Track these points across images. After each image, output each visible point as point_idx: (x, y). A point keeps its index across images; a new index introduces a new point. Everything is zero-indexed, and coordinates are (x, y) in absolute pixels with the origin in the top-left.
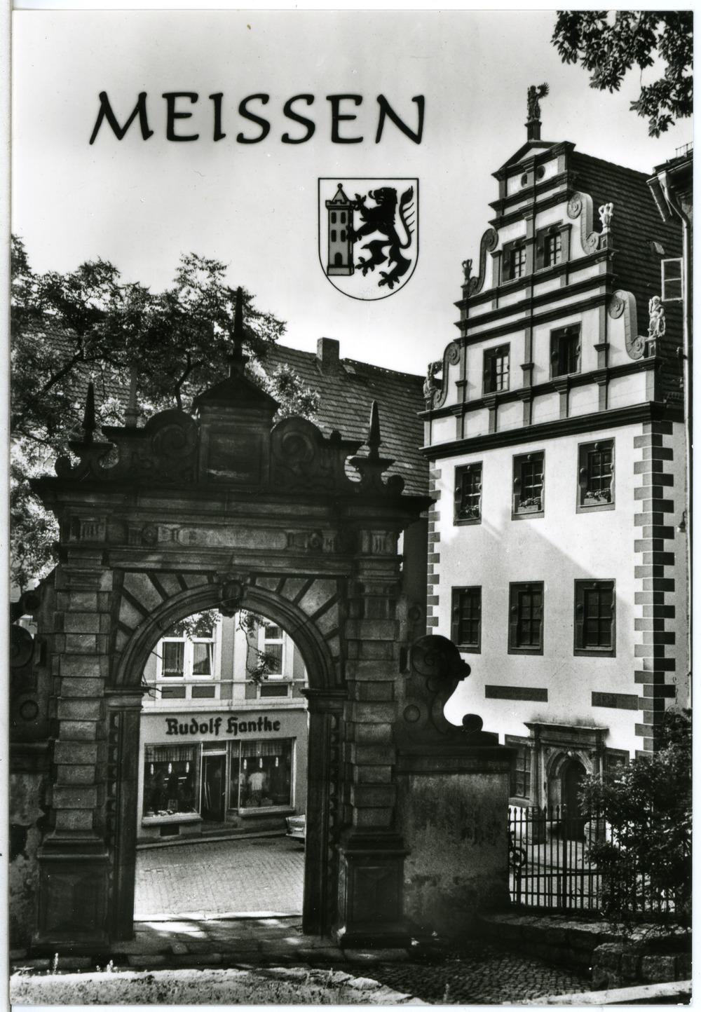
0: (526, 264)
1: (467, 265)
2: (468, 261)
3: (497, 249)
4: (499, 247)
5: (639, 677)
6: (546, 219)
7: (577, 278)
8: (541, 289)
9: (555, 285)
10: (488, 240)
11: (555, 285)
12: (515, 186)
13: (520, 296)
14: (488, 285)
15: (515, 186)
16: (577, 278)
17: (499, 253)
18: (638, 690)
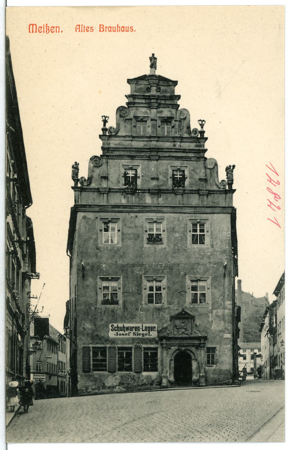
2: (107, 117)
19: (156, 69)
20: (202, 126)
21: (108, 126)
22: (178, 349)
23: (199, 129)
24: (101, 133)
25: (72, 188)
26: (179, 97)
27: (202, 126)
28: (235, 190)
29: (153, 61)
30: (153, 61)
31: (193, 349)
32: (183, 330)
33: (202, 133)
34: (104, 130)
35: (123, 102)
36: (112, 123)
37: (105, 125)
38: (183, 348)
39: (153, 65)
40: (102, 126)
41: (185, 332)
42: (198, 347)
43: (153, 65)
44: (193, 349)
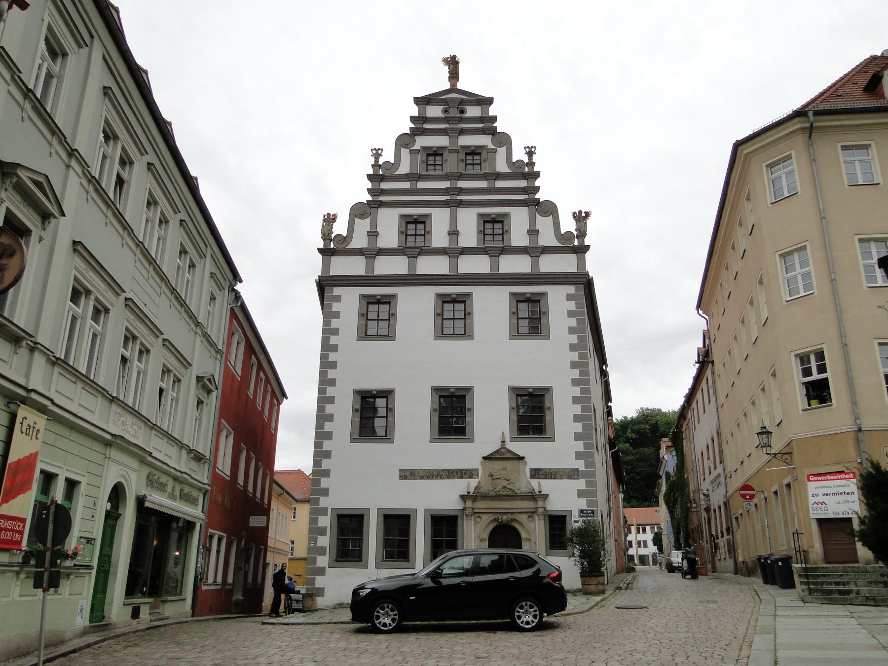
0: (452, 164)
1: (377, 154)
2: (379, 149)
3: (414, 148)
4: (416, 147)
5: (579, 456)
6: (466, 141)
7: (500, 184)
8: (462, 184)
9: (483, 184)
10: (403, 141)
11: (483, 184)
12: (435, 111)
13: (445, 184)
14: (404, 168)
15: (435, 111)
16: (500, 184)
17: (418, 151)
18: (580, 465)
19: (458, 81)
20: (530, 154)
21: (381, 161)
22: (496, 520)
23: (526, 160)
24: (371, 172)
25: (320, 251)
26: (494, 119)
27: (530, 154)
28: (587, 248)
29: (453, 63)
30: (453, 63)
31: (523, 518)
32: (505, 483)
33: (531, 164)
34: (376, 166)
35: (406, 127)
36: (388, 156)
37: (377, 160)
38: (505, 517)
39: (454, 75)
40: (372, 161)
41: (508, 486)
42: (532, 514)
43: (454, 75)
44: (523, 518)
